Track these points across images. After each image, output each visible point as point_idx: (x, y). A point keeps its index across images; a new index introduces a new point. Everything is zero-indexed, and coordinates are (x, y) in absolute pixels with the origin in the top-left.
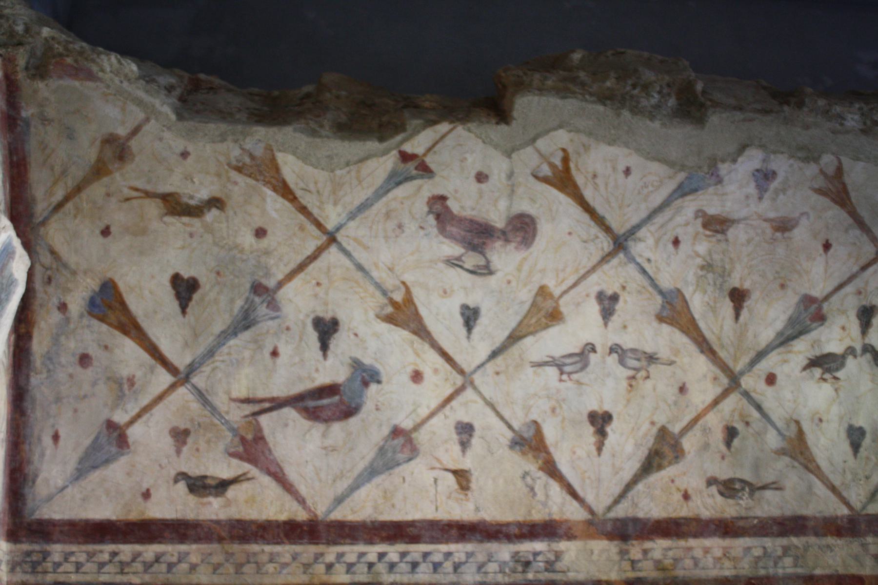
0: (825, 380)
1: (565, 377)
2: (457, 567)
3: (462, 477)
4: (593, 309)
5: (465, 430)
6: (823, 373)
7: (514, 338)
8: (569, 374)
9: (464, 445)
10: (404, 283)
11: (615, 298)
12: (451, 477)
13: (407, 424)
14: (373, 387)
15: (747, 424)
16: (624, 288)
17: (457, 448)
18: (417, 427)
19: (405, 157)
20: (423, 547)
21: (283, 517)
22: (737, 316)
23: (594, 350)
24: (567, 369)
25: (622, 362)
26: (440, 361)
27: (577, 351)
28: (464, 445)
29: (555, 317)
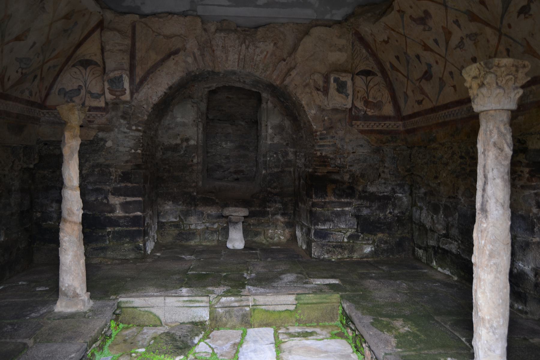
0: (527, 18)
1: (462, 50)
2: (457, 114)
3: (454, 87)
4: (455, 26)
5: (451, 73)
6: (525, 16)
7: (447, 43)
8: (462, 48)
9: (452, 78)
10: (421, 40)
11: (457, 21)
12: (452, 88)
13: (441, 76)
14: (432, 69)
15: (511, 45)
16: (457, 17)
17: (451, 79)
18: (443, 76)
19: (399, 11)
20: (451, 110)
21: (430, 107)
22: (487, 9)
23: (463, 39)
24: (461, 47)
25: (470, 39)
26: (438, 56)
27: (460, 40)
28: (452, 78)
29: (450, 33)
